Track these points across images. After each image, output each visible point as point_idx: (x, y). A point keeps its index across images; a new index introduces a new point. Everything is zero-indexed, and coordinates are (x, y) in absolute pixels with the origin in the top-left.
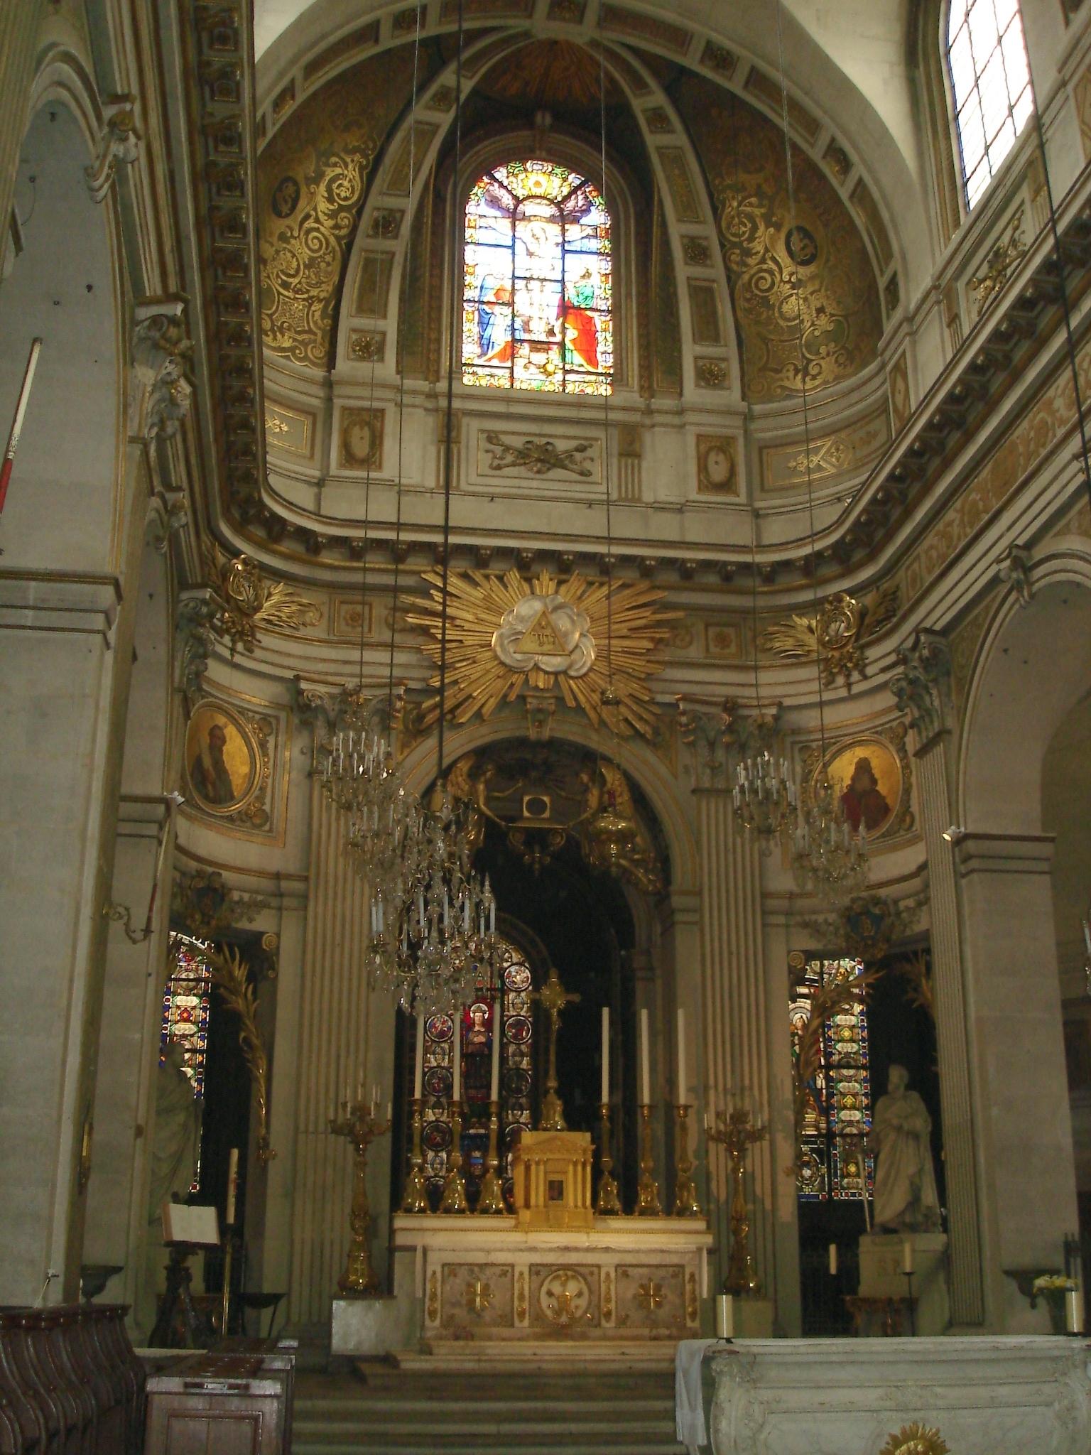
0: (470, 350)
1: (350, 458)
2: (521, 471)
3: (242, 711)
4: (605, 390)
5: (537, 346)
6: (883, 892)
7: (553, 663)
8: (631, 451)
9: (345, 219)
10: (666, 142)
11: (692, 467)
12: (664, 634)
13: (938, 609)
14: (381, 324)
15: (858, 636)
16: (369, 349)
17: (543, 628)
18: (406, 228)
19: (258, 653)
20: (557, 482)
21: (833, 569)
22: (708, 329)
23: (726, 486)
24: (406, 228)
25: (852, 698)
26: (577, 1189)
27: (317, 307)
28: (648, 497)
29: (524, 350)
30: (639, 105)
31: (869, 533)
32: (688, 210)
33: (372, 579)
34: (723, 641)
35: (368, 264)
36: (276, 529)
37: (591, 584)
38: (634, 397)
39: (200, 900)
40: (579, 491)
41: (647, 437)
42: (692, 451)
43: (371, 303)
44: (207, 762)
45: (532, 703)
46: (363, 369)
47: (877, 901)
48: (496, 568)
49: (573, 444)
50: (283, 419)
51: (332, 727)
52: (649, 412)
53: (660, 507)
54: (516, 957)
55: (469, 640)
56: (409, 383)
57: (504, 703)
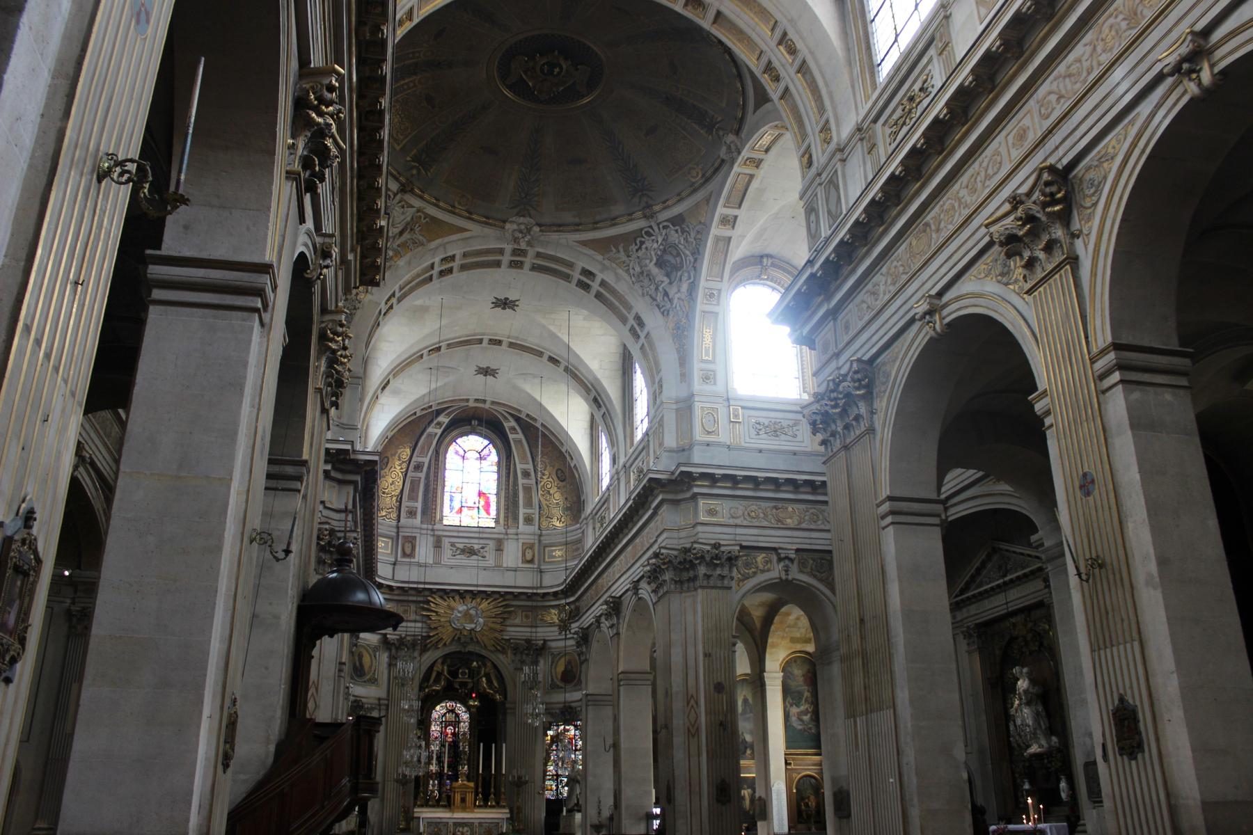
1: (404, 555)
4: (493, 525)
5: (469, 508)
7: (469, 626)
8: (499, 549)
9: (404, 466)
10: (516, 436)
13: (588, 619)
16: (412, 513)
17: (466, 614)
18: (425, 469)
22: (529, 504)
23: (531, 561)
24: (425, 469)
26: (470, 797)
29: (465, 510)
31: (572, 587)
34: (527, 617)
35: (412, 482)
38: (501, 529)
40: (482, 564)
43: (413, 497)
46: (410, 522)
47: (571, 707)
51: (397, 649)
53: (508, 569)
56: (425, 526)
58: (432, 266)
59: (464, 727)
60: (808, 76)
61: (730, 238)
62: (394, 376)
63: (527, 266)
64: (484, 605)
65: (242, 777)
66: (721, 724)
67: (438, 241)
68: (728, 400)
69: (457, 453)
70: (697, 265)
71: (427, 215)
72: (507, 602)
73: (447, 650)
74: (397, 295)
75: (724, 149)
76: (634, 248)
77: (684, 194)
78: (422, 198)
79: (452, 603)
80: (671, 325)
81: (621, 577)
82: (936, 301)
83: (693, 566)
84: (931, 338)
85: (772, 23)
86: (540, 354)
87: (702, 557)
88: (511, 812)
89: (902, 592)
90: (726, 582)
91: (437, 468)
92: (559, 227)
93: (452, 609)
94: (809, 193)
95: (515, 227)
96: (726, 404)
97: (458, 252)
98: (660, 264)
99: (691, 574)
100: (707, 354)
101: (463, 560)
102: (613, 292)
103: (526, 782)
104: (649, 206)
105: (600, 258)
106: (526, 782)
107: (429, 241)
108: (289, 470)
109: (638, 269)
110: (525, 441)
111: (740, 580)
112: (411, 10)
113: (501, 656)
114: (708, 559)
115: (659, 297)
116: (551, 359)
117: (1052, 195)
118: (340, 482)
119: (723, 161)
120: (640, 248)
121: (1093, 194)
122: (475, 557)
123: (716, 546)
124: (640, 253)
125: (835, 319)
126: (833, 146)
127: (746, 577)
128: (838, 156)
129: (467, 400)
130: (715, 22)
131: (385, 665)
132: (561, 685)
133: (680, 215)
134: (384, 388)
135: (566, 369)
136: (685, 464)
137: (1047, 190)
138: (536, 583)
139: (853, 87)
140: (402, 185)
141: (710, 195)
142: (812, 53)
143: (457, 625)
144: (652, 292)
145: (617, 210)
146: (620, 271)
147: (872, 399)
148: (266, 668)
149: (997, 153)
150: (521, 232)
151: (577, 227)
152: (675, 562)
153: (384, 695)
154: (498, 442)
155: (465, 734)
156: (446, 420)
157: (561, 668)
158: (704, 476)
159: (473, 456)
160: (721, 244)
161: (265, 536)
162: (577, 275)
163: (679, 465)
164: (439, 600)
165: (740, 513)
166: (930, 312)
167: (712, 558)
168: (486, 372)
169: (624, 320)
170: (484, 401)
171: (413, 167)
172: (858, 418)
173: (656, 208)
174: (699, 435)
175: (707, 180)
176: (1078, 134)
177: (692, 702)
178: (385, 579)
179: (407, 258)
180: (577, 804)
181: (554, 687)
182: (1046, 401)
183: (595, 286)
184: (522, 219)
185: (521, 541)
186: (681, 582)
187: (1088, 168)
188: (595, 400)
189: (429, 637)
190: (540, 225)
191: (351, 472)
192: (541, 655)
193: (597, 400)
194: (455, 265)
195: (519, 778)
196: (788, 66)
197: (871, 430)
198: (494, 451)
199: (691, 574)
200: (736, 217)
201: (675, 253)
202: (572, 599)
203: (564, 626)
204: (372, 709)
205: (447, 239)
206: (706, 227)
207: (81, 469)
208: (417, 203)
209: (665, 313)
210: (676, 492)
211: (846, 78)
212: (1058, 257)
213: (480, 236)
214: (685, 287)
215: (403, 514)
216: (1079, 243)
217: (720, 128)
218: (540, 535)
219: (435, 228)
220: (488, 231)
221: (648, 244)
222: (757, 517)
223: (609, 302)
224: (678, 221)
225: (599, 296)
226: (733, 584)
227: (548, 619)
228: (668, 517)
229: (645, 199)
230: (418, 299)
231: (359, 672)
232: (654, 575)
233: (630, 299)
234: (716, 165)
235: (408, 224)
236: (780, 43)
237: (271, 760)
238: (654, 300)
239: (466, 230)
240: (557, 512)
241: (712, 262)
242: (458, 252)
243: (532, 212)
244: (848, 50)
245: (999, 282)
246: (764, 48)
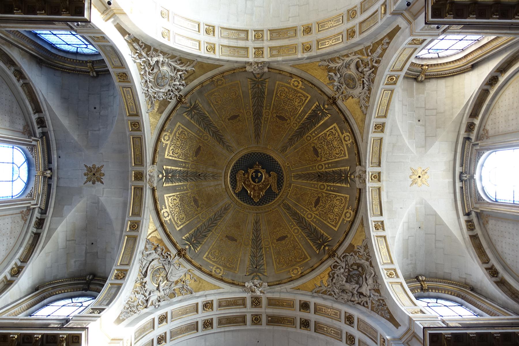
70: (373, 264)
75: (357, 179)
119: (360, 189)
120: (334, 278)
124: (334, 281)
141: (362, 219)
175: (356, 212)
201: (355, 267)
205: (207, 292)
208: (189, 266)
214: (370, 281)
221: (338, 272)
229: (327, 248)
239: (220, 288)
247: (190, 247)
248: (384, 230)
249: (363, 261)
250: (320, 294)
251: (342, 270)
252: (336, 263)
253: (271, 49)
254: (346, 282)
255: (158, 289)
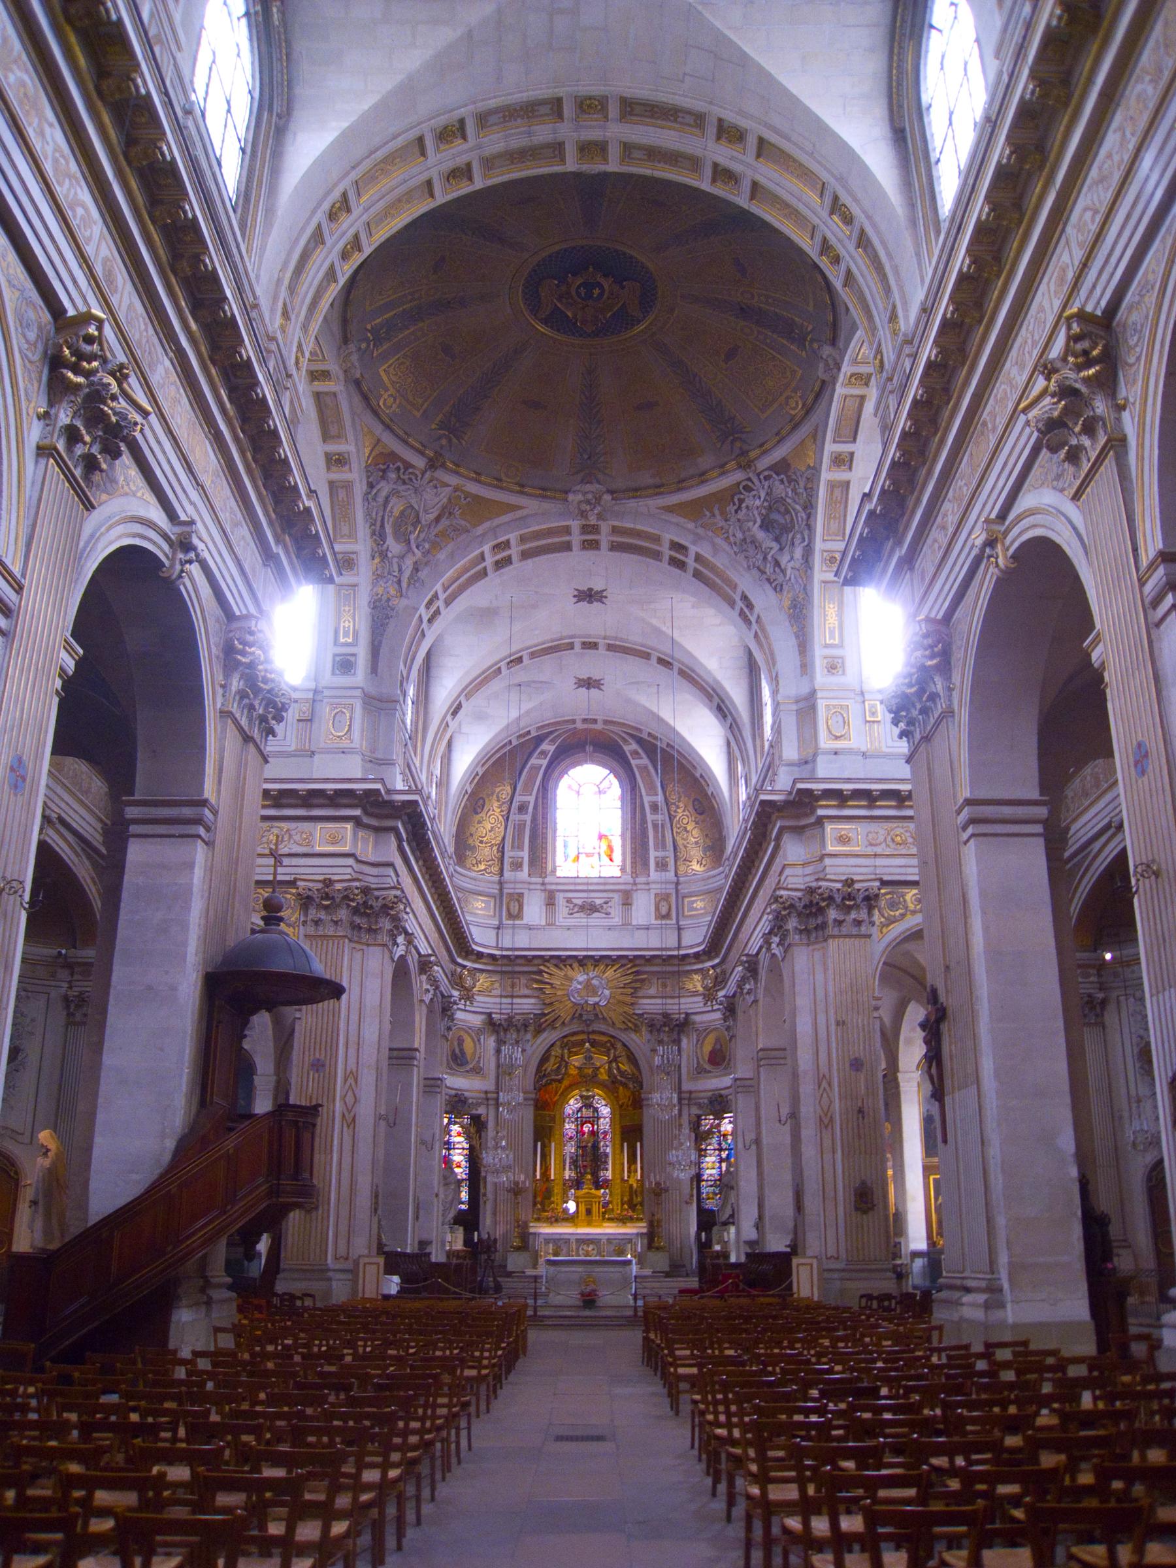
0: (559, 859)
2: (582, 915)
3: (470, 1028)
4: (619, 874)
5: (588, 855)
6: (723, 1092)
7: (592, 1000)
8: (627, 902)
9: (505, 808)
11: (653, 909)
12: (638, 985)
13: (731, 987)
14: (520, 854)
15: (715, 986)
16: (517, 866)
19: (475, 1004)
20: (596, 919)
21: (704, 958)
23: (667, 916)
25: (713, 1011)
27: (495, 848)
28: (634, 923)
29: (582, 857)
30: (626, 748)
32: (651, 790)
33: (517, 969)
34: (664, 986)
36: (480, 955)
37: (607, 966)
39: (457, 1105)
41: (635, 895)
42: (653, 901)
44: (457, 1051)
45: (585, 1017)
47: (721, 1096)
48: (569, 962)
49: (603, 901)
50: (482, 901)
51: (506, 1030)
52: (635, 884)
54: (604, 1103)
55: (559, 993)
56: (534, 880)
57: (573, 1018)
58: (482, 557)
59: (604, 1124)
60: (869, 250)
61: (848, 483)
62: (468, 697)
63: (604, 545)
64: (610, 973)
65: (134, 1177)
66: (860, 1111)
67: (487, 525)
68: (862, 693)
69: (570, 787)
71: (468, 495)
72: (637, 968)
73: (566, 1030)
74: (442, 596)
75: (821, 365)
76: (732, 508)
77: (783, 432)
78: (457, 473)
79: (570, 973)
80: (787, 603)
81: (754, 929)
82: (996, 527)
83: (821, 911)
84: (998, 578)
85: (819, 186)
86: (646, 656)
87: (831, 898)
88: (651, 1225)
89: (986, 929)
90: (863, 929)
91: (545, 806)
92: (636, 492)
93: (571, 980)
94: (882, 406)
95: (580, 497)
96: (859, 699)
97: (513, 537)
98: (766, 525)
99: (820, 920)
100: (832, 637)
101: (581, 919)
102: (712, 568)
103: (666, 1190)
104: (744, 453)
105: (691, 526)
106: (666, 1190)
107: (475, 526)
108: (187, 812)
109: (739, 535)
110: (651, 764)
111: (883, 925)
112: (356, 237)
113: (634, 1036)
114: (838, 900)
115: (769, 569)
116: (661, 661)
117: (1086, 353)
118: (377, 830)
119: (823, 382)
120: (739, 508)
121: (1136, 345)
122: (596, 915)
123: (849, 883)
124: (741, 515)
125: (911, 569)
126: (901, 338)
127: (891, 921)
128: (907, 350)
129: (574, 721)
130: (752, 197)
131: (492, 1052)
132: (708, 1067)
133: (784, 460)
134: (455, 713)
135: (681, 673)
136: (802, 780)
137: (1079, 347)
138: (672, 942)
139: (918, 254)
140: (430, 460)
142: (869, 217)
143: (576, 999)
144: (760, 563)
145: (706, 461)
146: (719, 541)
147: (950, 669)
148: (162, 1050)
149: (1041, 309)
150: (588, 502)
151: (658, 489)
152: (800, 906)
153: (492, 1088)
154: (621, 771)
155: (605, 1133)
156: (552, 748)
157: (708, 1048)
158: (828, 794)
159: (589, 791)
160: (837, 492)
161: (14, 884)
162: (667, 552)
163: (795, 781)
164: (554, 970)
165: (881, 838)
166: (991, 543)
167: (844, 899)
168: (589, 683)
169: (732, 604)
170: (595, 721)
171: (440, 438)
172: (933, 697)
173: (752, 454)
174: (825, 742)
175: (808, 411)
176: (1113, 260)
177: (824, 1084)
178: (484, 946)
179: (450, 547)
180: (732, 1216)
181: (700, 1071)
182: (1099, 649)
183: (690, 561)
184: (588, 487)
185: (653, 892)
186: (807, 931)
187: (1130, 308)
188: (719, 708)
189: (545, 1015)
190: (612, 492)
191: (387, 817)
192: (683, 1031)
193: (722, 709)
194: (514, 551)
195: (658, 1184)
196: (847, 242)
197: (949, 713)
198: (616, 783)
199: (820, 920)
200: (852, 454)
201: (782, 509)
202: (717, 961)
203: (709, 995)
204: (479, 1105)
205: (496, 522)
206: (816, 470)
207: (51, 832)
208: (454, 480)
209: (778, 589)
210: (798, 817)
211: (908, 242)
212: (1102, 439)
213: (539, 514)
215: (506, 867)
216: (1126, 415)
217: (812, 341)
218: (677, 884)
219: (479, 510)
220: (547, 505)
221: (749, 502)
222: (904, 843)
223: (709, 580)
224: (782, 468)
225: (697, 575)
226: (874, 931)
227: (690, 986)
228: (793, 851)
229: (738, 444)
230: (477, 596)
231: (458, 1060)
232: (778, 926)
233: (733, 575)
234: (816, 388)
235: (444, 508)
236: (832, 213)
237: (167, 1157)
238: (763, 572)
239: (519, 508)
240: (696, 853)
241: (829, 517)
242: (513, 537)
243: (600, 476)
244: (912, 206)
245: (1054, 488)
246: (816, 221)
247: (450, 441)
248: (850, 468)
249: (797, 507)
250: (710, 534)
251: (758, 503)
252: (750, 484)
253: (628, 148)
254: (761, 527)
255: (410, 550)
